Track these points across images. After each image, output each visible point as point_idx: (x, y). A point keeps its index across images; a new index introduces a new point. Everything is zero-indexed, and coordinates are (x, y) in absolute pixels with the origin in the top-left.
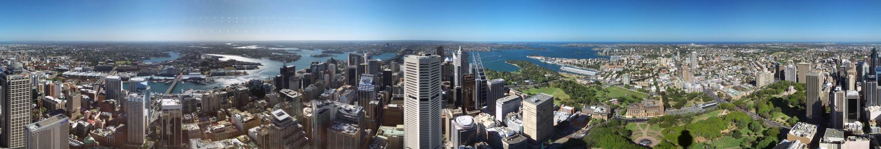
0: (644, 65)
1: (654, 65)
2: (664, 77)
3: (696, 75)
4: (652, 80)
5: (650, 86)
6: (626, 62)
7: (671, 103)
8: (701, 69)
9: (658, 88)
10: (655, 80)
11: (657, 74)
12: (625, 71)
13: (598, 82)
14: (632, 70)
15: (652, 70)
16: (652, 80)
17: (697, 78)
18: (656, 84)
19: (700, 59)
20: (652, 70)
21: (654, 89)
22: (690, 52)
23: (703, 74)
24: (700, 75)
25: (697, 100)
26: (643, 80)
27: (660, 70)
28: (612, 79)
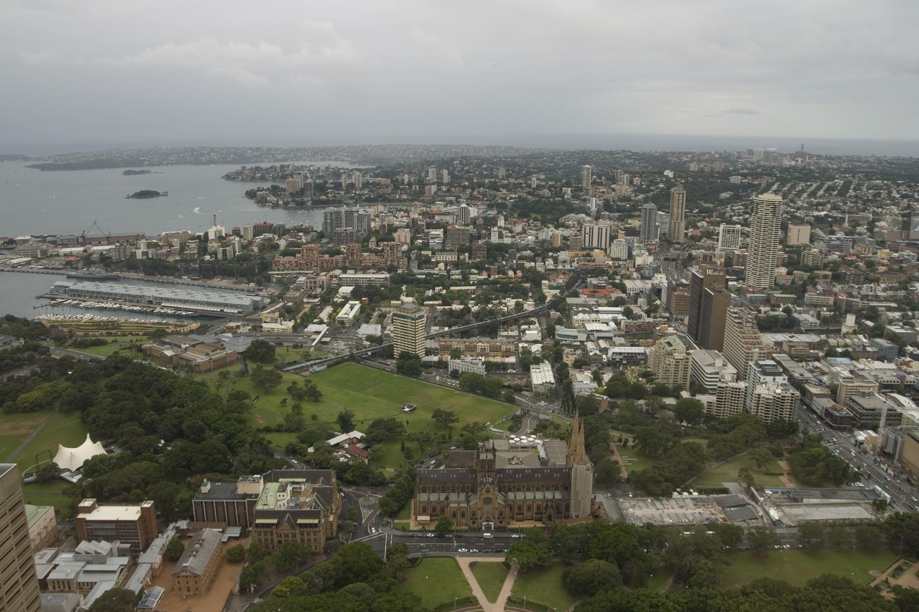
0: (497, 252)
1: (543, 250)
2: (597, 322)
3: (768, 325)
4: (533, 333)
5: (527, 362)
6: (403, 236)
7: (626, 464)
8: (799, 291)
9: (562, 374)
10: (549, 332)
11: (558, 304)
12: (401, 282)
13: (261, 352)
14: (430, 282)
15: (536, 278)
16: (533, 333)
17: (769, 339)
18: (554, 355)
19: (799, 235)
20: (536, 278)
21: (543, 375)
22: (740, 193)
23: (808, 318)
24: (790, 325)
25: (761, 462)
26: (491, 331)
27: (576, 281)
28: (337, 328)
